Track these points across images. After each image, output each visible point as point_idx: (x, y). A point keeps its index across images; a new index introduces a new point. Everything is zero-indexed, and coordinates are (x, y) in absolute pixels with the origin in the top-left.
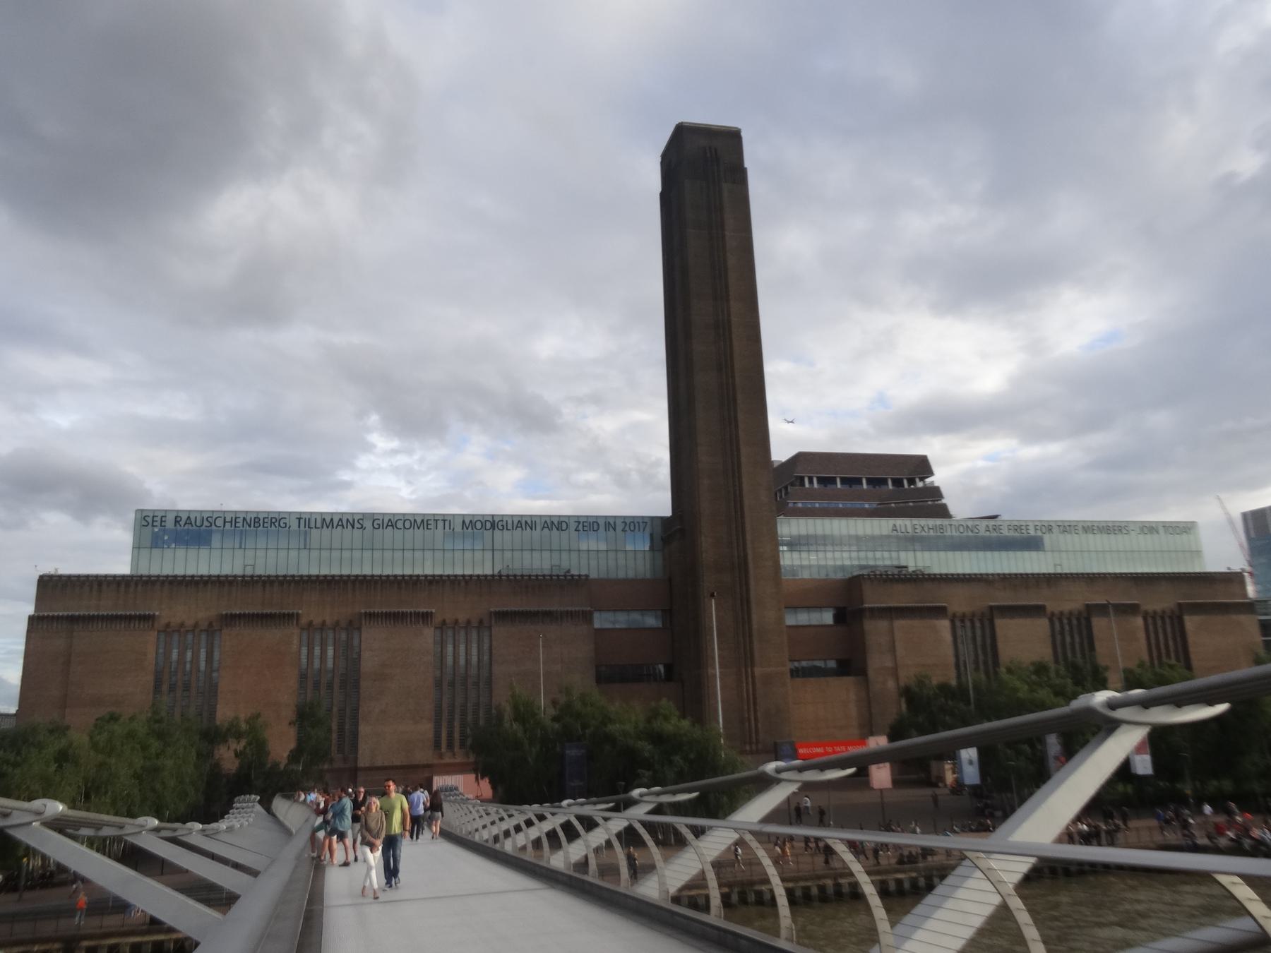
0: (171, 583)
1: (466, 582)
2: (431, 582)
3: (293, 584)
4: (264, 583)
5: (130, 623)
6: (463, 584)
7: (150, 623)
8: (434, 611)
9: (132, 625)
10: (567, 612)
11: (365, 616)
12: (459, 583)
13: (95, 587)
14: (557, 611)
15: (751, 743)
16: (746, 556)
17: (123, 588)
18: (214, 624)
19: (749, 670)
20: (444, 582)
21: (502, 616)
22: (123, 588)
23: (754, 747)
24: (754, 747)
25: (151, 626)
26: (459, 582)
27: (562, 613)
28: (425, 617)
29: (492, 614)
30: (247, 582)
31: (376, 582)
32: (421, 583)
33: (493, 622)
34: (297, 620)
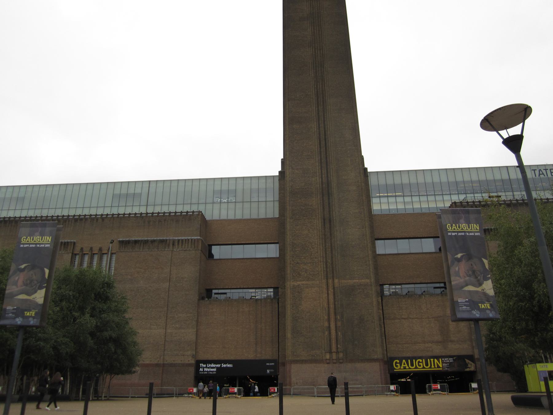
1: (103, 219)
2: (76, 220)
6: (100, 220)
8: (75, 241)
10: (179, 240)
14: (170, 240)
15: (331, 352)
16: (329, 183)
19: (330, 281)
20: (86, 219)
21: (124, 244)
23: (334, 356)
24: (334, 356)
26: (97, 219)
27: (174, 241)
32: (69, 221)
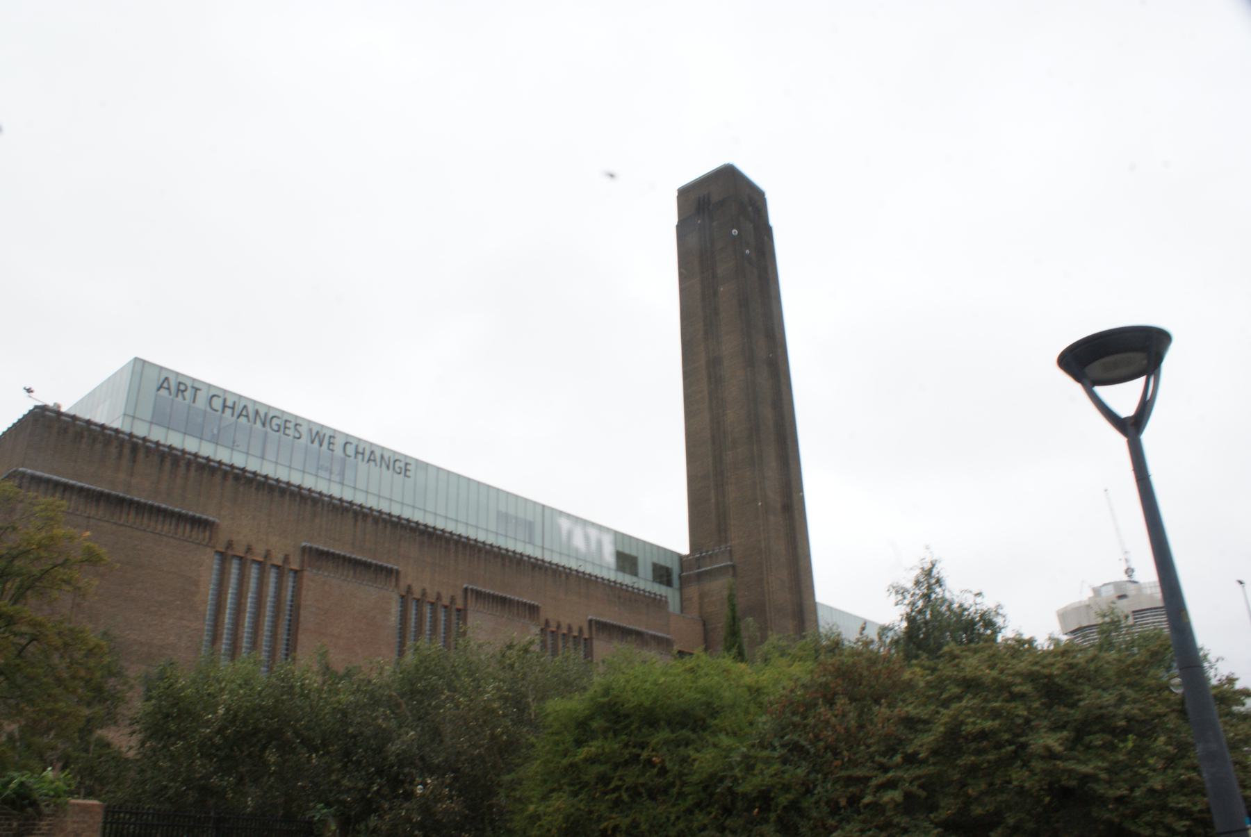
0: (237, 478)
3: (389, 526)
4: (356, 513)
5: (177, 525)
6: (564, 576)
7: (207, 534)
9: (180, 530)
11: (472, 594)
12: (560, 576)
13: (127, 451)
17: (168, 465)
18: (291, 559)
22: (168, 465)
25: (207, 540)
28: (533, 610)
29: (593, 622)
30: (334, 506)
31: (480, 550)
33: (594, 633)
34: (397, 580)
